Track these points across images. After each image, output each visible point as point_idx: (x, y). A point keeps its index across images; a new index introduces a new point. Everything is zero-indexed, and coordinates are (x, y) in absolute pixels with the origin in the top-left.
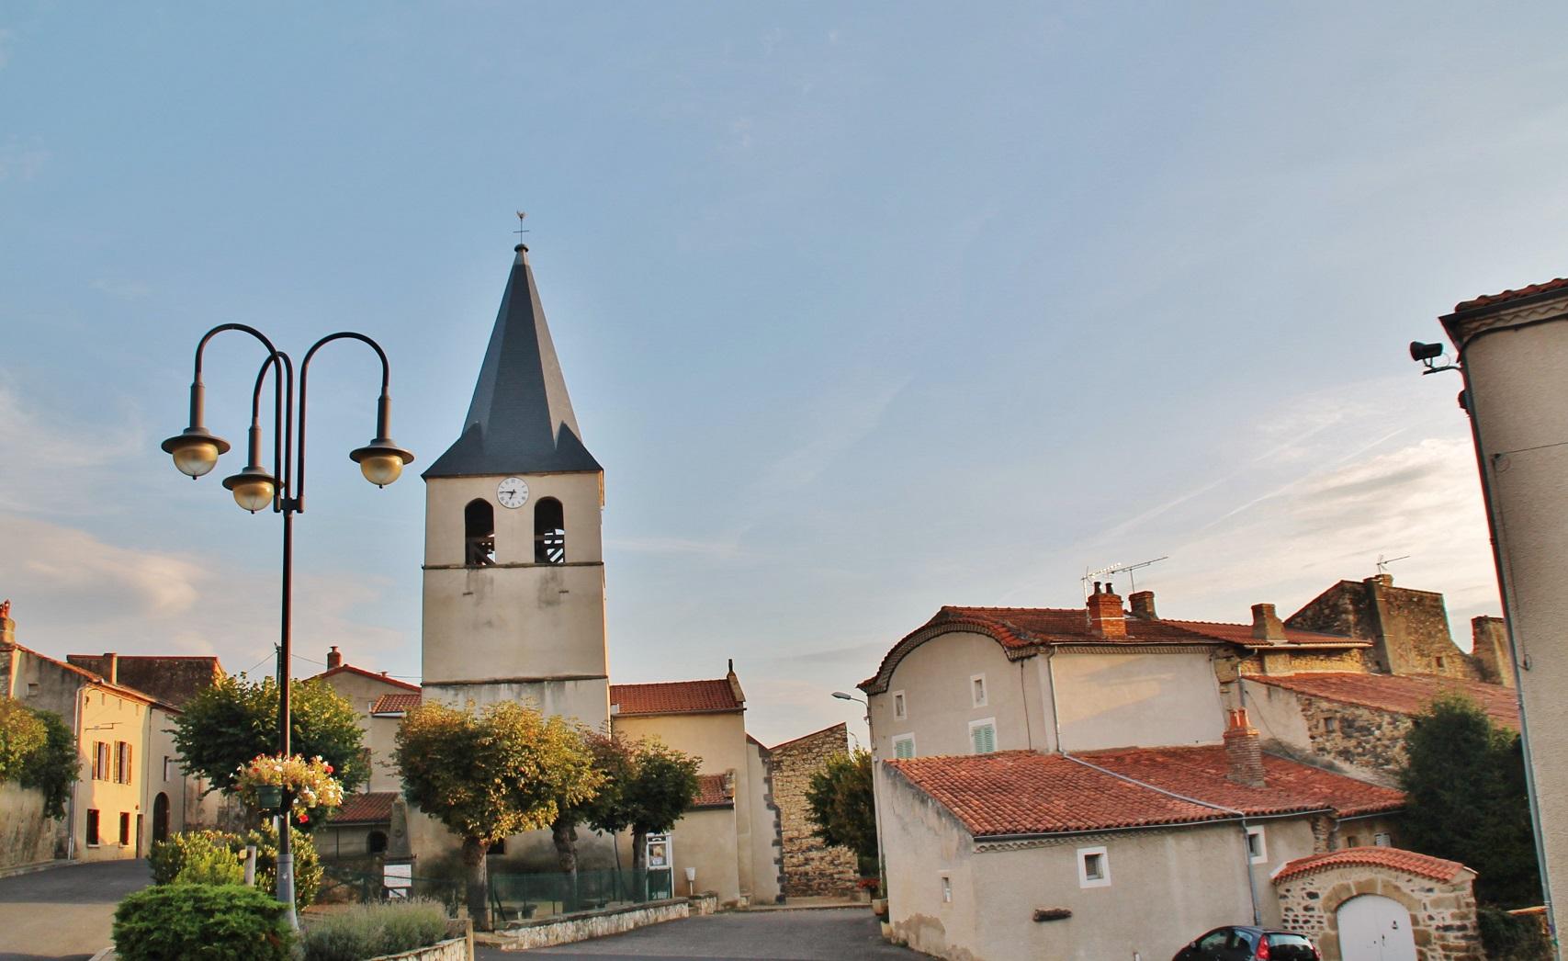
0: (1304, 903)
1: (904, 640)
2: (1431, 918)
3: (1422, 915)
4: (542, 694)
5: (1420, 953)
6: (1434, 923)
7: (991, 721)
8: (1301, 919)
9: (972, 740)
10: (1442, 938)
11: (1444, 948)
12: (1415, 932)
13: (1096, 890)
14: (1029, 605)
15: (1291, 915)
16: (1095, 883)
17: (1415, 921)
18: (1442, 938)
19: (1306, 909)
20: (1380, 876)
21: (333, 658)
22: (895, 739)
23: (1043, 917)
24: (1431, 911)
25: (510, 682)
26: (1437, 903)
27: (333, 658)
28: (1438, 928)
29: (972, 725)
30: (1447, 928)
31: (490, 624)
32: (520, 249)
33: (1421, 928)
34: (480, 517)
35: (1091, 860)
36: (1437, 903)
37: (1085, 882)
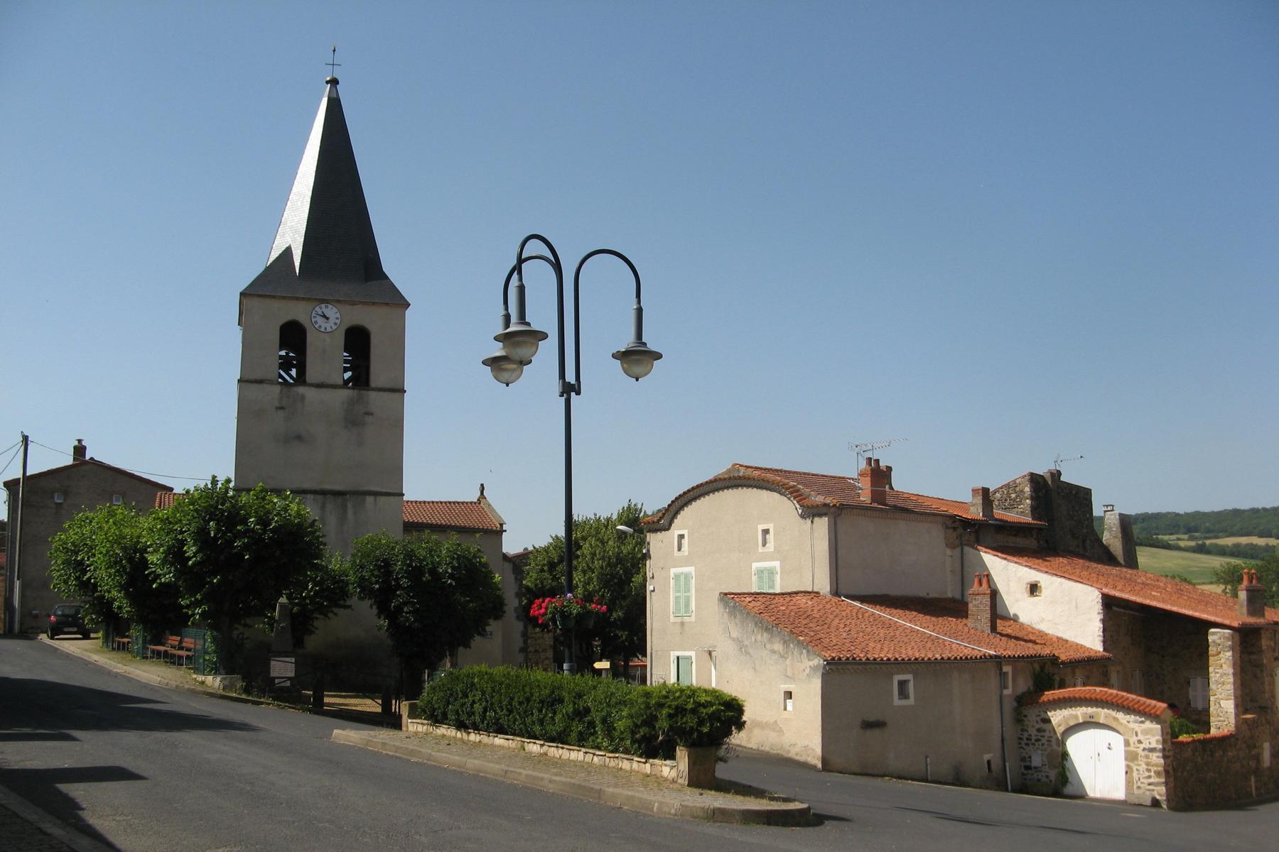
0: (1037, 726)
1: (689, 491)
2: (1140, 742)
3: (1133, 739)
4: (344, 508)
5: (1128, 766)
6: (1142, 746)
7: (777, 564)
8: (1033, 738)
9: (754, 578)
10: (1147, 757)
11: (1147, 764)
12: (1126, 752)
13: (904, 707)
14: (1216, 509)
15: (1026, 735)
16: (904, 702)
17: (1127, 743)
18: (1147, 757)
19: (1039, 730)
20: (1102, 714)
21: (80, 450)
22: (673, 571)
23: (868, 725)
24: (1140, 737)
25: (315, 492)
26: (1145, 732)
27: (80, 450)
28: (1144, 749)
29: (755, 565)
30: (1152, 750)
31: (299, 438)
32: (334, 82)
33: (1132, 748)
34: (293, 336)
35: (902, 684)
36: (1145, 732)
37: (897, 701)
